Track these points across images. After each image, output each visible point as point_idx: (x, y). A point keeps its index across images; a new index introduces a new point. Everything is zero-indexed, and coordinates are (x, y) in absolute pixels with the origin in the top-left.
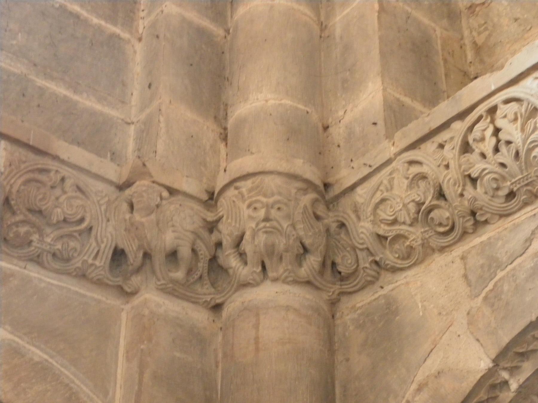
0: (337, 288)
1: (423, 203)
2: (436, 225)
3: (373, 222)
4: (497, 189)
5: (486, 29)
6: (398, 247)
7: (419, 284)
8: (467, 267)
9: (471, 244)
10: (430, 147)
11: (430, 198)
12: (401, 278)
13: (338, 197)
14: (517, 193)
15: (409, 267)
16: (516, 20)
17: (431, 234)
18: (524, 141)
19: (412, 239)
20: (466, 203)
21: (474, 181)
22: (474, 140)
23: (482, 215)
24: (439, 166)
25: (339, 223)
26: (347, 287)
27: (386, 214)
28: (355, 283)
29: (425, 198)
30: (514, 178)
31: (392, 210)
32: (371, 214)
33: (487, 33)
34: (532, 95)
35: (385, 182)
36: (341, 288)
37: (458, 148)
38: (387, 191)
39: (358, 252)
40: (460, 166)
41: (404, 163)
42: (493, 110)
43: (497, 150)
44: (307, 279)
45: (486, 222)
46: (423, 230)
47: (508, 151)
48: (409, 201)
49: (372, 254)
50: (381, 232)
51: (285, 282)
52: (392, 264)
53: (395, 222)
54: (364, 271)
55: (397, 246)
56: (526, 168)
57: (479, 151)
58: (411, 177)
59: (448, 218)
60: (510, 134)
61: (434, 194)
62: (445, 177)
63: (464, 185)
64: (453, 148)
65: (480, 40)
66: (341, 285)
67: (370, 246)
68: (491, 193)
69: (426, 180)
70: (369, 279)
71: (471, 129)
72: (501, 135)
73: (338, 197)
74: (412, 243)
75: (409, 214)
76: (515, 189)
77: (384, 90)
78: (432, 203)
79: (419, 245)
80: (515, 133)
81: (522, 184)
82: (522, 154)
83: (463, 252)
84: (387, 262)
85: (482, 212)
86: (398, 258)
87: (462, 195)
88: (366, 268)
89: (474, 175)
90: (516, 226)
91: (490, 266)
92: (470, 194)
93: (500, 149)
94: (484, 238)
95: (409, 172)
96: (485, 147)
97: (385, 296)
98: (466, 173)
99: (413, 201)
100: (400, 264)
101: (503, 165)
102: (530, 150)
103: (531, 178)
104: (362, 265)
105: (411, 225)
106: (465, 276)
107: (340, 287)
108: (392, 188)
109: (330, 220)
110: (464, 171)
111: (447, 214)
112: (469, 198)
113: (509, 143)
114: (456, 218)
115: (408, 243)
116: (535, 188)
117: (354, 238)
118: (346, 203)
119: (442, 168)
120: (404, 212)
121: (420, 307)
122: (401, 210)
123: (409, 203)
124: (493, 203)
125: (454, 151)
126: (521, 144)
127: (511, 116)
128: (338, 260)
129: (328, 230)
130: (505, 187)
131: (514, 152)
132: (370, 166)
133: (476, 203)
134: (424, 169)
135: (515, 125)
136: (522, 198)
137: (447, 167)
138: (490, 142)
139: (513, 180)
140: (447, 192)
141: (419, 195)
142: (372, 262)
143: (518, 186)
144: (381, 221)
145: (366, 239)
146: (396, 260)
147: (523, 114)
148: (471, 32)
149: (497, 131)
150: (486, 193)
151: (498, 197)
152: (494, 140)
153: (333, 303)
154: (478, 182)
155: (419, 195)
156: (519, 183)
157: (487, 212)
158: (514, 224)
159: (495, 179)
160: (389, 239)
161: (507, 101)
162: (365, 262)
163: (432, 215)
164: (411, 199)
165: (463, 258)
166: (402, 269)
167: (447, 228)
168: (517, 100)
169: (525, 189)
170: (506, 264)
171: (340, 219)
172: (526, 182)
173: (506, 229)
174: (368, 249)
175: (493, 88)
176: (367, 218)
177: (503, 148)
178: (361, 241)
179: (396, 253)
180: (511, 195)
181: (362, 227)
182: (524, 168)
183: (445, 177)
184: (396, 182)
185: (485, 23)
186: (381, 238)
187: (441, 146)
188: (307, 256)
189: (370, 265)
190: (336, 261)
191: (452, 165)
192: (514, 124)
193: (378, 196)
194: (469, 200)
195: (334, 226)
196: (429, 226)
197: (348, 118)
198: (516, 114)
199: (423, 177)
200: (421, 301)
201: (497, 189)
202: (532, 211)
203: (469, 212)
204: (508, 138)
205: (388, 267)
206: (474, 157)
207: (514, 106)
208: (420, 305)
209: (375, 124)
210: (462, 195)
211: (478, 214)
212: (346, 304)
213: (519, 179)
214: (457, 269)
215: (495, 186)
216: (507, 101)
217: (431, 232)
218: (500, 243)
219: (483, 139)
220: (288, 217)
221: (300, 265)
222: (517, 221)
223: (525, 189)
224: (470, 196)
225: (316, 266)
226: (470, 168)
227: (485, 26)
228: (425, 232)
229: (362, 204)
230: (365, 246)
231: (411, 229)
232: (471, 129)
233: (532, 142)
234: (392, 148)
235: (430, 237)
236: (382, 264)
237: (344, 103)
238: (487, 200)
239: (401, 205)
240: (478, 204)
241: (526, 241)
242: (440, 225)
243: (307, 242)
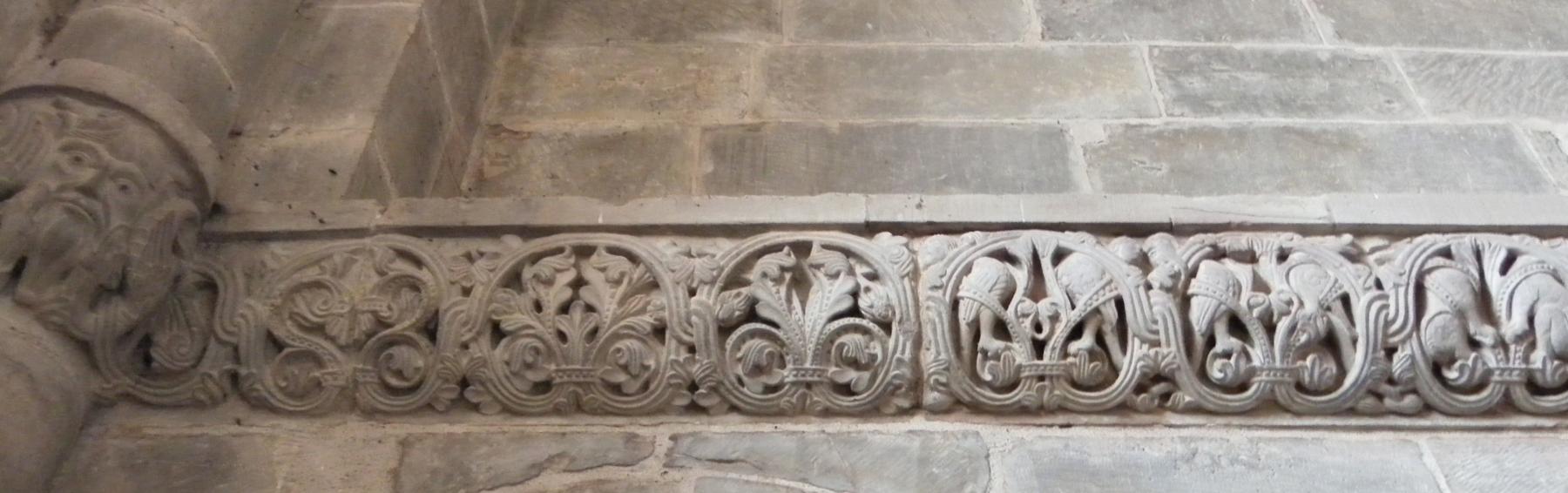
0: (126, 382)
1: (389, 326)
2: (389, 369)
3: (276, 311)
4: (529, 366)
5: (506, 164)
6: (296, 372)
7: (295, 448)
8: (407, 460)
9: (430, 429)
10: (452, 248)
11: (407, 323)
12: (262, 425)
13: (227, 238)
14: (554, 389)
15: (291, 414)
16: (553, 177)
17: (370, 380)
18: (616, 320)
19: (330, 370)
20: (465, 361)
21: (497, 333)
22: (536, 276)
23: (478, 393)
24: (453, 283)
25: (204, 279)
26: (147, 392)
27: (311, 307)
28: (166, 391)
29: (400, 320)
30: (567, 364)
31: (324, 308)
32: (281, 295)
33: (504, 169)
34: (661, 263)
35: (337, 259)
36: (132, 387)
37: (500, 274)
38: (334, 274)
39: (213, 344)
40: (490, 301)
41: (390, 248)
42: (584, 252)
43: (565, 309)
44: (87, 338)
45: (476, 408)
46: (361, 366)
47: (582, 321)
48: (366, 308)
49: (237, 359)
50: (280, 333)
51: (43, 319)
52: (265, 394)
53: (319, 329)
54: (203, 381)
55: (294, 369)
56: (595, 360)
57: (534, 296)
58: (392, 274)
59: (417, 369)
60: (598, 296)
61: (418, 320)
62: (455, 304)
63: (479, 333)
64: (491, 271)
65: (491, 172)
66: (138, 382)
67: (243, 345)
68: (516, 367)
69: (416, 293)
70: (202, 397)
71: (535, 258)
72: (584, 292)
73: (227, 238)
74: (326, 376)
75: (351, 329)
76: (558, 380)
77: (372, 136)
78: (408, 333)
79: (335, 387)
80: (607, 299)
81: (574, 379)
82: (603, 337)
83: (410, 434)
84: (258, 386)
85: (481, 389)
86: (281, 389)
87: (465, 346)
88: (210, 376)
89: (505, 326)
90: (523, 438)
91: (449, 477)
92: (481, 351)
93: (571, 310)
94: (459, 429)
95: (392, 266)
96: (547, 294)
97: (213, 440)
98: (495, 317)
99: (374, 313)
100: (279, 400)
101: (562, 336)
102: (617, 336)
103: (592, 376)
104: (205, 367)
105: (342, 348)
106: (395, 474)
107: (133, 384)
108: (342, 275)
109: (192, 266)
110: (493, 312)
111: (420, 363)
112: (476, 356)
113: (590, 309)
114: (432, 378)
115: (317, 374)
116: (586, 395)
117: (221, 317)
118: (240, 255)
119: (456, 290)
120: (344, 323)
121: (279, 487)
122: (342, 316)
123: (363, 312)
124: (508, 385)
125: (491, 275)
126: (608, 321)
127: (614, 274)
128: (162, 338)
129: (177, 279)
130: (544, 368)
131: (592, 326)
132: (321, 221)
133: (482, 369)
134: (424, 274)
135: (613, 290)
136: (557, 400)
137: (467, 292)
138: (557, 294)
139: (564, 367)
140: (446, 331)
141: (390, 308)
142: (228, 371)
143: (566, 379)
144: (292, 316)
145: (244, 331)
146: (274, 390)
147: (634, 281)
148: (482, 155)
149: (578, 283)
150: (507, 363)
151: (523, 378)
152: (568, 293)
153: (99, 405)
154: (504, 342)
155: (390, 308)
156: (569, 376)
157: (489, 392)
158: (523, 432)
159: (537, 351)
160: (287, 351)
161: (614, 251)
162: (216, 364)
163: (395, 350)
164: (372, 308)
165: (404, 444)
166: (274, 411)
167: (405, 384)
168: (633, 258)
169: (572, 388)
170: (481, 487)
171: (212, 273)
172: (582, 379)
173: (504, 433)
174: (236, 349)
175: (600, 221)
176: (268, 297)
177: (577, 314)
178: (232, 329)
179: (286, 379)
180: (544, 387)
181: (249, 306)
182: (592, 357)
183: (455, 304)
184: (355, 269)
185: (508, 156)
186: (275, 344)
187: (469, 258)
188: (116, 299)
189: (221, 375)
190: (156, 339)
191: (478, 291)
192: (611, 287)
193: (312, 274)
194: (472, 359)
195: (191, 278)
196: (376, 365)
197: (283, 141)
198: (623, 275)
199: (415, 286)
200: (285, 478)
201: (529, 366)
202: (561, 425)
203: (459, 379)
204: (593, 301)
205: (255, 394)
206: (525, 300)
207: (622, 263)
208: (280, 484)
209: (333, 172)
210: (465, 346)
211: (471, 387)
212: (123, 416)
213: (574, 370)
214: (387, 455)
215: (530, 359)
216: (614, 251)
217: (372, 377)
218: (484, 450)
219: (549, 282)
220: (131, 212)
221: (93, 306)
222: (529, 429)
223: (572, 388)
224: (480, 355)
225: (121, 326)
226: (505, 312)
227: (505, 160)
228: (363, 370)
229: (272, 271)
230: (233, 340)
231: (338, 354)
232: (535, 258)
233: (626, 327)
234: (378, 216)
235: (365, 383)
236: (245, 385)
237: (288, 116)
238: (501, 374)
239: (346, 309)
240: (484, 373)
241: (533, 466)
242: (399, 374)
243: (135, 275)
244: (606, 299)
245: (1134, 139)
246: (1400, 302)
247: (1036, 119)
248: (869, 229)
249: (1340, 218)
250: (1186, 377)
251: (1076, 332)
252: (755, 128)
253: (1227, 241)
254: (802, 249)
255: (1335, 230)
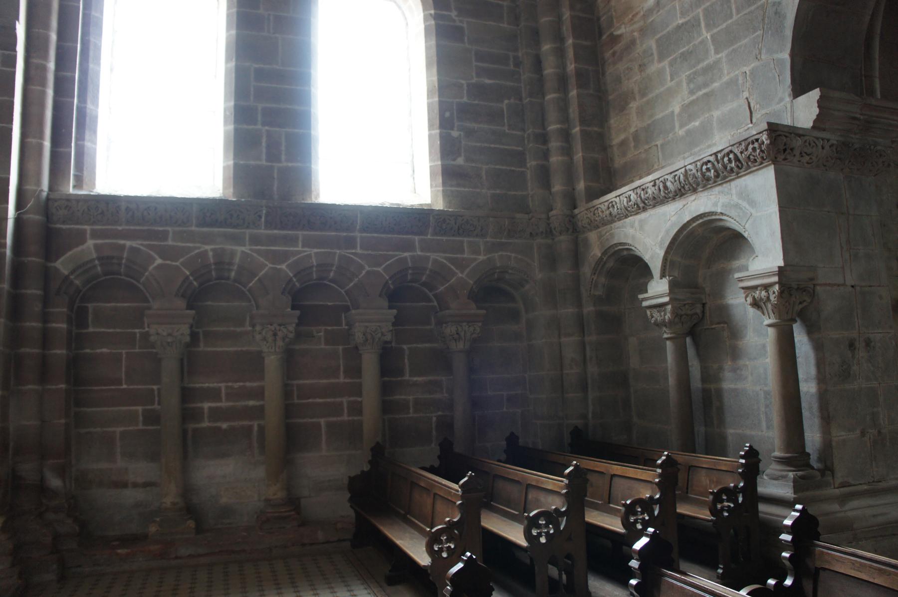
244: (600, 214)
245: (685, 108)
246: (658, 191)
247: (670, 110)
248: (616, 197)
249: (653, 179)
250: (646, 206)
251: (635, 205)
252: (637, 131)
253: (643, 187)
254: (612, 202)
255: (652, 181)
